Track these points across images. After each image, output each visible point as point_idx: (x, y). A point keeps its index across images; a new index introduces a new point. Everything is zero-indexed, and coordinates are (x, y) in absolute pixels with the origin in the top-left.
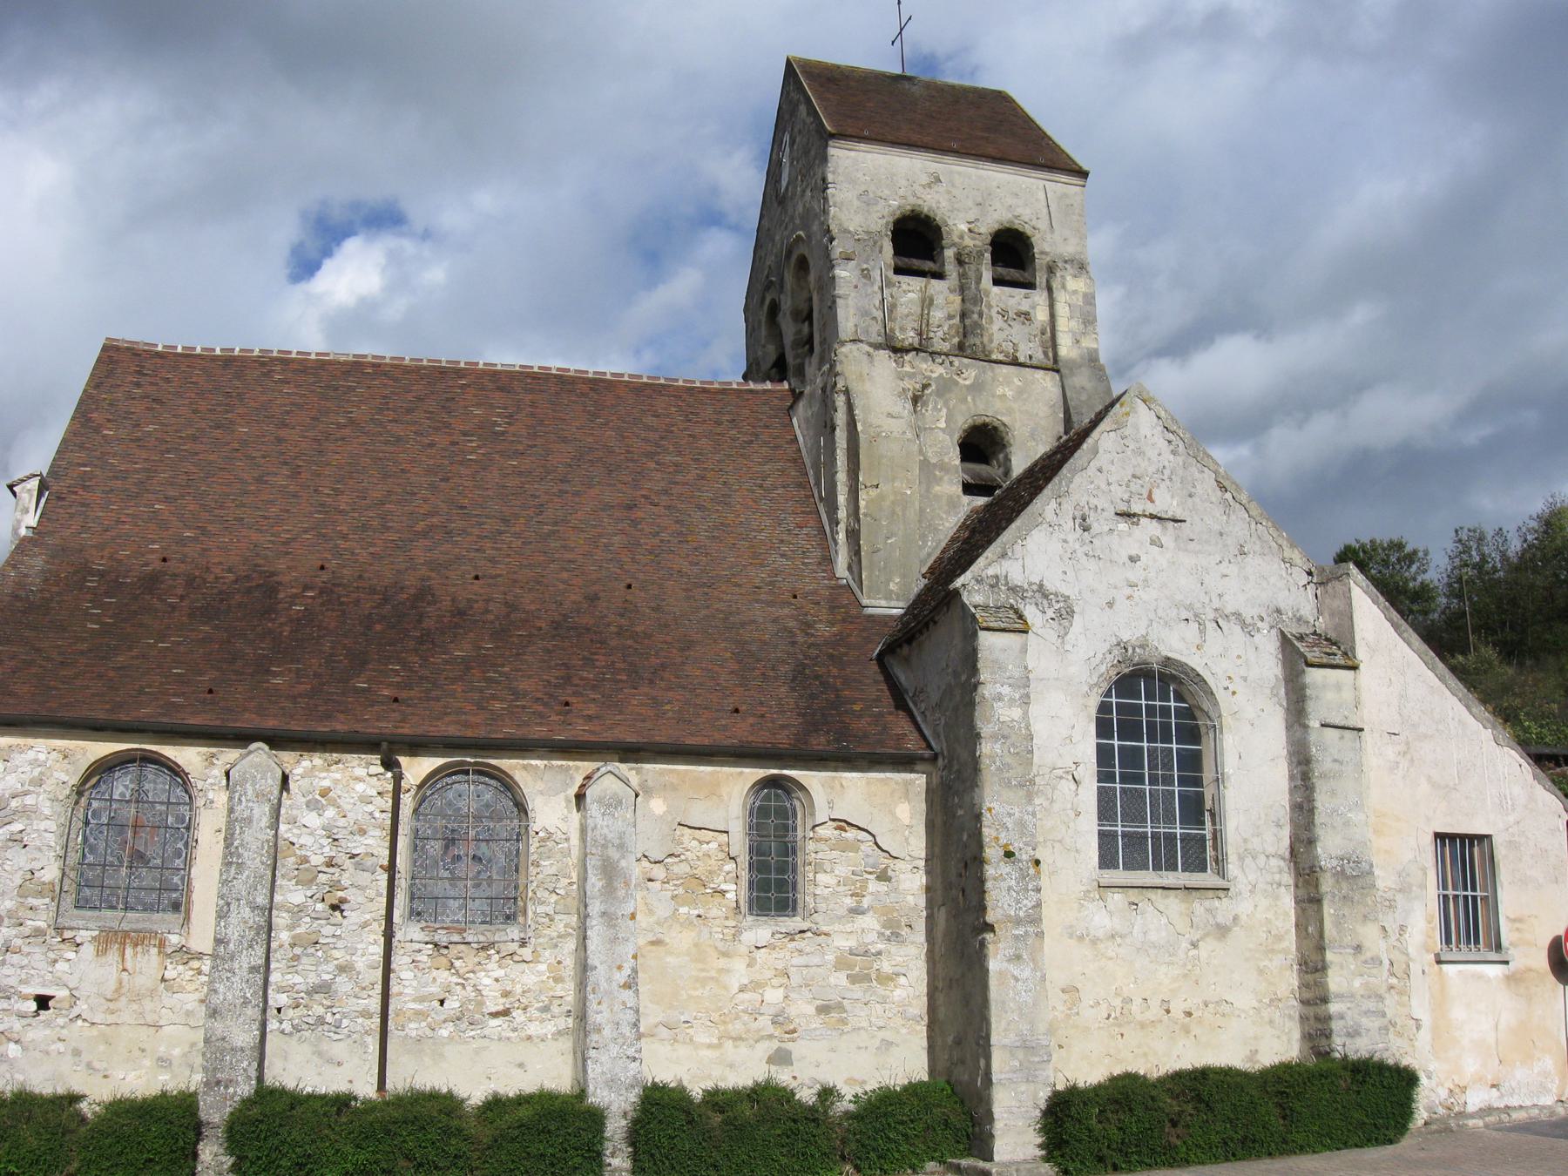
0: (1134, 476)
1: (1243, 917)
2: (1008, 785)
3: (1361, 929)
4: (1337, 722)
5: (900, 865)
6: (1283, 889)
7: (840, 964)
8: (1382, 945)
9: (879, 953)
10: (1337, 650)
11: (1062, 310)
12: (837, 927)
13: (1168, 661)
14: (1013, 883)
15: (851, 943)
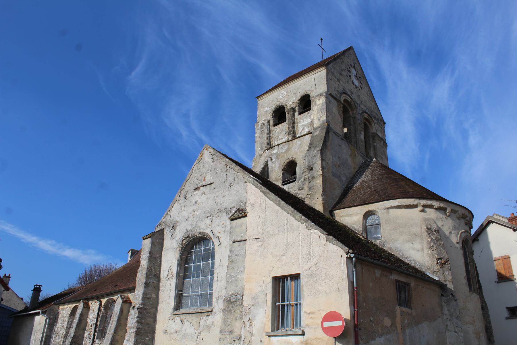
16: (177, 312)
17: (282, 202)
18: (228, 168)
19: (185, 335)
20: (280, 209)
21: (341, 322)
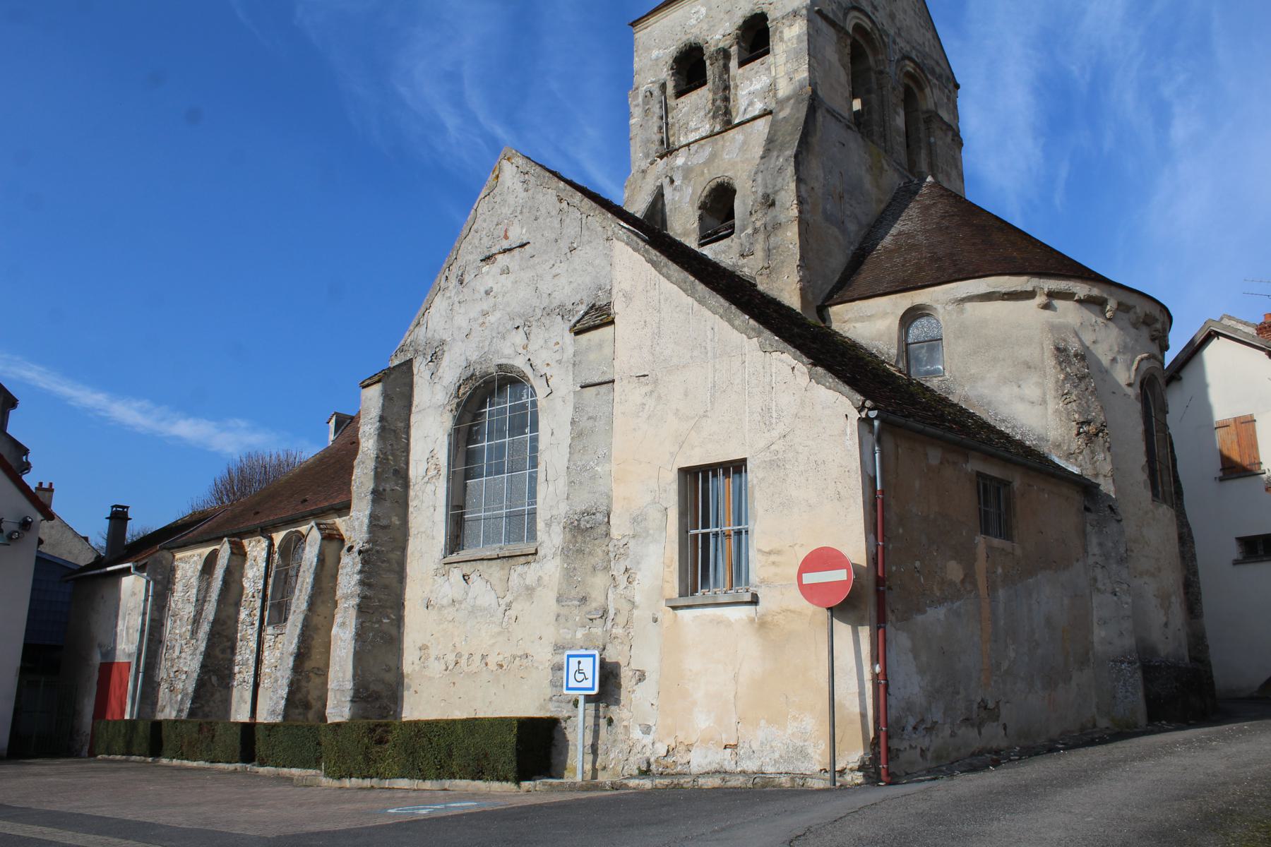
4: (596, 380)
16: (454, 557)
17: (700, 287)
18: (564, 204)
19: (474, 611)
21: (844, 572)
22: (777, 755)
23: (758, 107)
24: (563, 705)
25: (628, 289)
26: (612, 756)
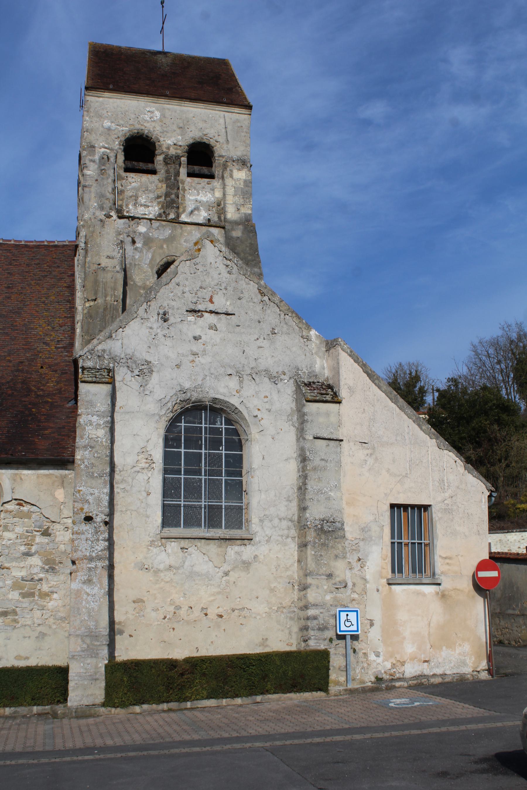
0: (201, 288)
1: (261, 557)
2: (92, 477)
3: (333, 563)
4: (325, 436)
5: (57, 526)
6: (289, 540)
7: (16, 586)
8: (348, 574)
9: (41, 580)
10: (326, 392)
11: (230, 191)
12: (14, 564)
13: (215, 400)
14: (90, 536)
15: (23, 573)
17: (401, 400)
19: (192, 575)
20: (397, 409)
21: (497, 572)
22: (452, 665)
23: (202, 216)
24: (321, 641)
25: (351, 385)
26: (357, 671)
